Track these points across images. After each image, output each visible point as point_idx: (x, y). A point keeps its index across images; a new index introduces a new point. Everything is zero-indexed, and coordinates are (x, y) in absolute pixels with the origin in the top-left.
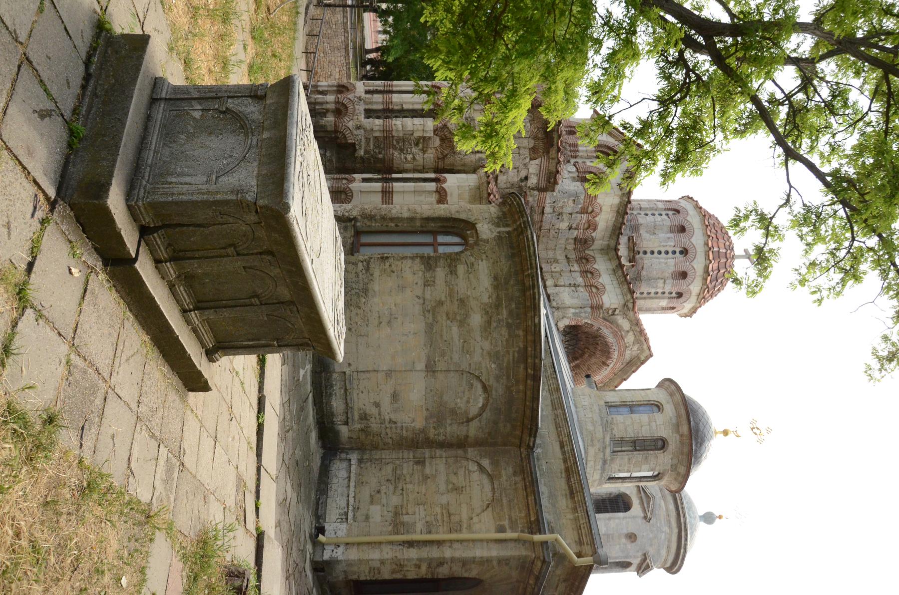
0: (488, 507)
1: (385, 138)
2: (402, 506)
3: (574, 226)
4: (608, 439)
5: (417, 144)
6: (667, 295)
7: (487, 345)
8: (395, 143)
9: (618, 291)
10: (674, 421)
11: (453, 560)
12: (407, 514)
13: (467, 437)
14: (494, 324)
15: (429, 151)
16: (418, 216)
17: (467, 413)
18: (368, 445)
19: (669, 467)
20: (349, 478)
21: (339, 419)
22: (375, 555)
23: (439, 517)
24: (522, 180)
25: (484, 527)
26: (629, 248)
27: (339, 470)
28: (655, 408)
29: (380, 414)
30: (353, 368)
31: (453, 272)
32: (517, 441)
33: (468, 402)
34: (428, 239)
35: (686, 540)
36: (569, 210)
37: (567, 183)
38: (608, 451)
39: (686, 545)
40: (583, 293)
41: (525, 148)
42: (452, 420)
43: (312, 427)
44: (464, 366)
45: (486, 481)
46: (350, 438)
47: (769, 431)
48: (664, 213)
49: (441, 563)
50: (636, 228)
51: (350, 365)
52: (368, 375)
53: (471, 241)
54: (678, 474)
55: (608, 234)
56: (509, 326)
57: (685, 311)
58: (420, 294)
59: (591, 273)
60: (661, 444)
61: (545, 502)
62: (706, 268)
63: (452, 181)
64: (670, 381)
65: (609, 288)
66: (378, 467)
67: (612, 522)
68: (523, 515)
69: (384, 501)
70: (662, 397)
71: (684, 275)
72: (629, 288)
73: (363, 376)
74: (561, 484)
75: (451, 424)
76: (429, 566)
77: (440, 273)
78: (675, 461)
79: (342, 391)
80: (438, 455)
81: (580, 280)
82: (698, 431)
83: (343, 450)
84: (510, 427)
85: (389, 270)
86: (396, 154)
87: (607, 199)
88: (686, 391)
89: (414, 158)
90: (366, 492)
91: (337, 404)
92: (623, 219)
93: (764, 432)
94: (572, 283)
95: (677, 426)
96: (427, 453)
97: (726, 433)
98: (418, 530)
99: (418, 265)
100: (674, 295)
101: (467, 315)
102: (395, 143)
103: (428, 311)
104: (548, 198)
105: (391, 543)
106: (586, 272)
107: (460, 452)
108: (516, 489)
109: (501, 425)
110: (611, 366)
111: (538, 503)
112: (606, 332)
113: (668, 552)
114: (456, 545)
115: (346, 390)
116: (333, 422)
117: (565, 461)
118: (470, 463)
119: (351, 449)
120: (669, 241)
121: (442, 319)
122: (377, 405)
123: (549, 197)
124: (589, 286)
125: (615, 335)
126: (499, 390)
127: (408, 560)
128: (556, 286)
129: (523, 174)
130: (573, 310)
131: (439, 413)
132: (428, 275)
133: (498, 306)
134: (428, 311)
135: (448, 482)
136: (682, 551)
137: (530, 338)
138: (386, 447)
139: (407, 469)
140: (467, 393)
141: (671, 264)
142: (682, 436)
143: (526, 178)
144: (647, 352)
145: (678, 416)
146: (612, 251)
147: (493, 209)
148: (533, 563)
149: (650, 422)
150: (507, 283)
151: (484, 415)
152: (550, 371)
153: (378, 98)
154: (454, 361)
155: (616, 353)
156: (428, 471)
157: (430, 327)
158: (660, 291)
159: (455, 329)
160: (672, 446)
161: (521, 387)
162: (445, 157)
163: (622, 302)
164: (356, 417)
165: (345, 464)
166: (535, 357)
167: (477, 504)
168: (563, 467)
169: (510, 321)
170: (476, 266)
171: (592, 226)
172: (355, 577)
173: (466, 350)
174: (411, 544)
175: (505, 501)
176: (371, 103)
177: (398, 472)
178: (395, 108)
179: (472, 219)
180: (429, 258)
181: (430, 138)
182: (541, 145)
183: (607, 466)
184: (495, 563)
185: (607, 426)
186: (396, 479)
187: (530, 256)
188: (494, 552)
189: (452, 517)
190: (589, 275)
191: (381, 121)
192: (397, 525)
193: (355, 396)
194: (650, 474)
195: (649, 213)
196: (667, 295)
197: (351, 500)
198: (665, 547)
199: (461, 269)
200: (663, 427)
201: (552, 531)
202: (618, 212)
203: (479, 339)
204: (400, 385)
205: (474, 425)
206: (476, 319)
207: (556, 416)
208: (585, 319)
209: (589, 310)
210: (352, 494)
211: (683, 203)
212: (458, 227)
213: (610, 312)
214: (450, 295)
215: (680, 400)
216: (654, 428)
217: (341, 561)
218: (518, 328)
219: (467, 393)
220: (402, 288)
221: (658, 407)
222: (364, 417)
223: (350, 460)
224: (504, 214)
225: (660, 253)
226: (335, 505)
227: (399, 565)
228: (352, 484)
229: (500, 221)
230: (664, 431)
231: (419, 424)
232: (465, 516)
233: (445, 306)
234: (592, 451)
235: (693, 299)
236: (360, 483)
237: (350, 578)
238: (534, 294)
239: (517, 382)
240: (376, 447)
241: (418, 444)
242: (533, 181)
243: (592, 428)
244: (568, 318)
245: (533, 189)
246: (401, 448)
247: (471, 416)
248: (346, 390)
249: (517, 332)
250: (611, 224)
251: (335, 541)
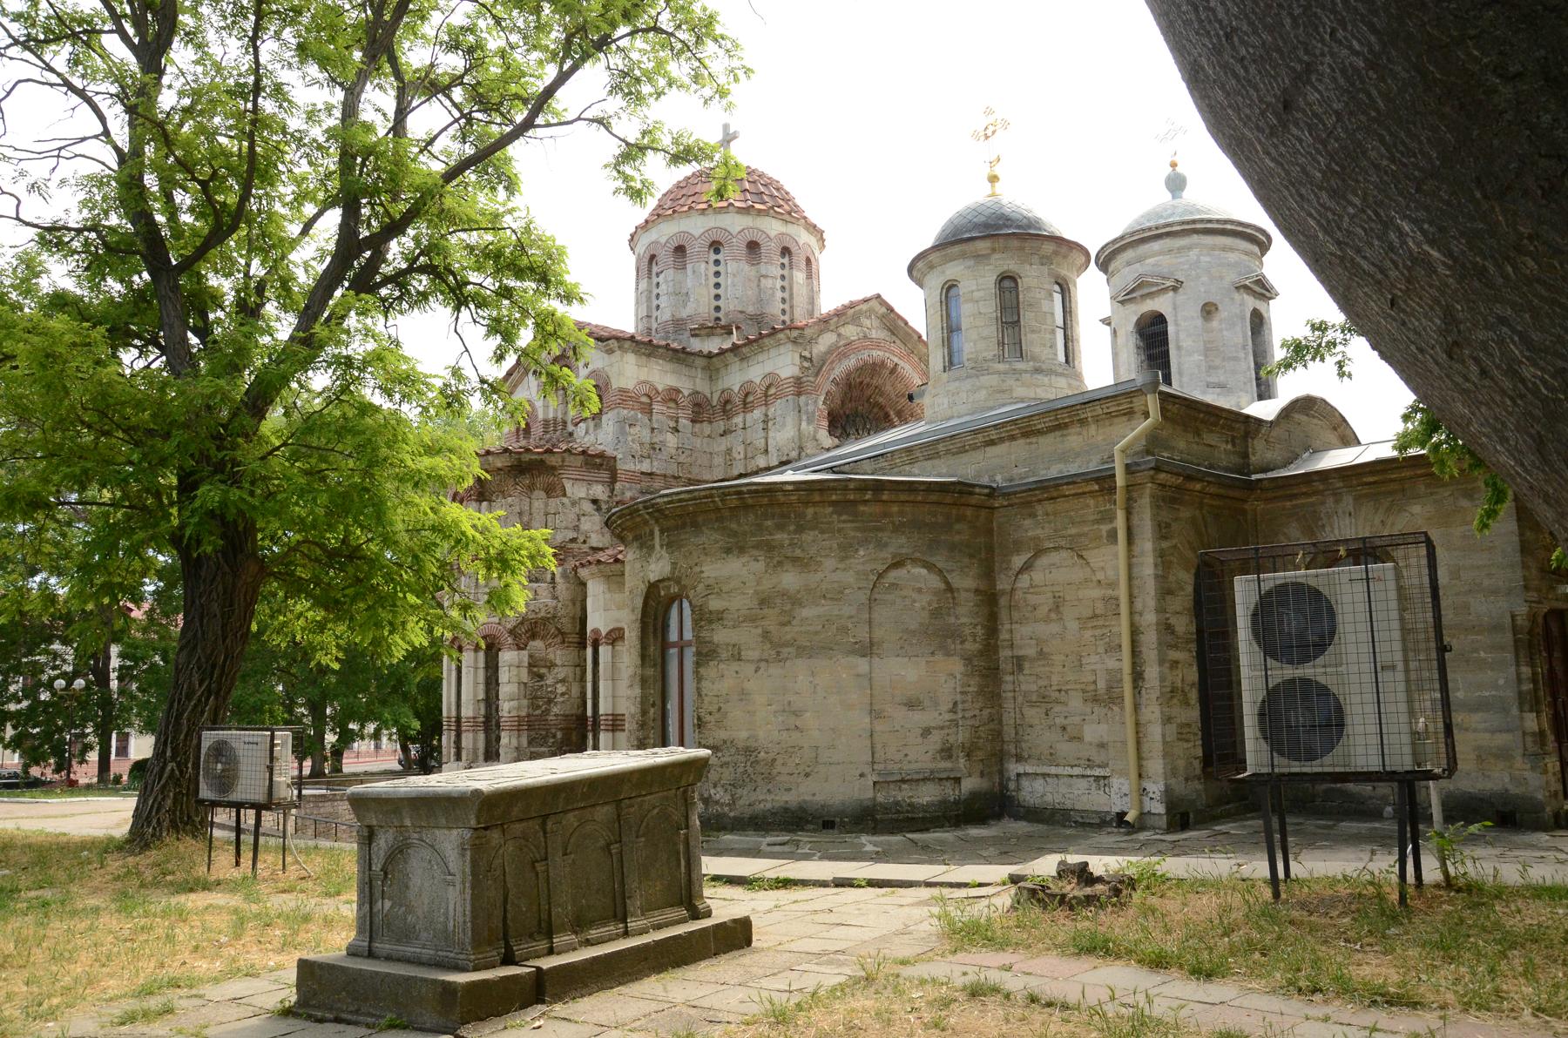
0: (1081, 557)
1: (530, 728)
2: (1084, 691)
3: (672, 424)
4: (1001, 367)
5: (541, 677)
6: (786, 272)
7: (829, 563)
8: (538, 712)
9: (773, 352)
10: (971, 262)
11: (1160, 610)
12: (1095, 682)
13: (977, 591)
14: (798, 552)
15: (551, 656)
16: (639, 671)
17: (936, 593)
18: (994, 746)
19: (1045, 268)
20: (1044, 775)
21: (950, 793)
22: (1155, 732)
23: (1098, 632)
24: (599, 509)
25: (1110, 560)
26: (708, 335)
27: (1034, 792)
28: (953, 292)
29: (942, 728)
30: (867, 770)
31: (719, 617)
32: (983, 513)
33: (920, 590)
34: (674, 651)
35: (1210, 221)
36: (645, 435)
37: (602, 438)
38: (1020, 366)
39: (1218, 221)
40: (777, 408)
41: (547, 505)
43: (959, 833)
44: (862, 597)
45: (1044, 561)
46: (982, 775)
47: (989, 111)
48: (655, 280)
49: (1166, 628)
50: (678, 324)
51: (862, 775)
52: (879, 747)
53: (674, 589)
54: (1056, 253)
55: (685, 370)
56: (800, 529)
57: (812, 241)
58: (752, 667)
59: (747, 395)
60: (1008, 283)
61: (1073, 469)
62: (740, 211)
63: (597, 621)
64: (911, 269)
65: (768, 369)
66: (1029, 730)
67: (1184, 345)
68: (1092, 502)
69: (1077, 719)
70: (936, 281)
71: (753, 246)
72: (768, 335)
73: (879, 755)
74: (1046, 443)
75: (957, 617)
76: (1175, 647)
77: (721, 635)
78: (1035, 259)
80: (1007, 637)
81: (757, 414)
82: (986, 226)
83: (1003, 787)
84: (964, 524)
85: (717, 716)
86: (555, 710)
87: (629, 372)
88: (928, 242)
89: (563, 681)
90: (1065, 749)
91: (927, 795)
92: (659, 346)
93: (991, 119)
94: (762, 425)
95: (979, 258)
96: (1005, 653)
97: (993, 179)
98: (1116, 665)
99: (709, 671)
100: (786, 261)
101: (784, 594)
102: (538, 712)
103: (778, 653)
104: (626, 467)
105: (1137, 707)
106: (745, 403)
107: (1003, 601)
108: (1055, 514)
109: (957, 538)
110: (896, 360)
111: (1072, 480)
112: (839, 370)
113: (1232, 249)
114: (1138, 605)
115: (903, 781)
116: (957, 802)
117: (1012, 438)
118: (1019, 585)
119: (1001, 772)
120: (698, 274)
121: (789, 633)
122: (926, 732)
123: (625, 465)
124: (767, 399)
125: (844, 355)
126: (900, 544)
127: (1162, 679)
128: (766, 451)
129: (588, 507)
130: (804, 424)
131: (939, 634)
132: (724, 655)
133: (770, 548)
134: (778, 653)
135: (1047, 620)
136: (1229, 227)
137: (817, 497)
138: (996, 719)
139: (1028, 684)
140: (904, 593)
141: (735, 268)
142: (994, 250)
143: (595, 502)
144: (874, 303)
145: (963, 256)
146: (712, 363)
147: (630, 555)
148: (1163, 486)
149: (972, 300)
150: (735, 534)
151: (940, 565)
152: (882, 463)
153: (467, 740)
154: (853, 613)
155: (875, 353)
156: (1031, 652)
157: (803, 651)
158: (779, 283)
159: (806, 612)
160: (1010, 264)
161: (895, 509)
162: (560, 632)
163: (790, 346)
164: (948, 764)
165: (1025, 783)
166: (846, 489)
167: (1078, 574)
168: (1021, 441)
169: (792, 528)
170: (711, 582)
171: (672, 396)
172: (1197, 765)
173: (837, 595)
174: (1137, 676)
175: (1073, 531)
176: (475, 750)
177: (1034, 698)
178: (483, 712)
179: (643, 588)
180: (698, 653)
181: (531, 656)
182: (541, 480)
184: (1165, 545)
185: (979, 369)
186: (1043, 700)
187: (695, 499)
188: (1146, 546)
189: (1098, 612)
190: (750, 398)
191: (503, 734)
192: (1111, 698)
193: (914, 766)
194: (1058, 298)
195: (655, 303)
196: (786, 272)
197: (1077, 771)
198: (1223, 254)
199: (715, 604)
200: (981, 281)
201: (1111, 458)
202: (649, 355)
203: (820, 575)
205: (956, 580)
206: (790, 579)
207: (948, 452)
208: (818, 405)
209: (803, 399)
210: (1068, 771)
211: (641, 249)
212: (655, 609)
213: (806, 364)
214: (754, 621)
215: (938, 254)
216: (981, 294)
217: (1166, 785)
218: (802, 516)
219: (904, 593)
220: (744, 695)
221: (950, 287)
222: (947, 752)
223: (1019, 775)
224: (636, 538)
225: (717, 285)
226: (1083, 796)
227: (1172, 694)
228: (1053, 770)
229: (645, 544)
230: (990, 279)
231: (957, 666)
232: (1096, 593)
233: (771, 628)
234: (1020, 391)
235: (791, 229)
236: (1053, 759)
237: (1198, 771)
238: (750, 492)
239: (885, 515)
240: (998, 735)
241: (990, 668)
242: (599, 491)
243: (984, 392)
244: (816, 432)
245: (612, 491)
246: (999, 696)
247: (943, 586)
248: (903, 781)
249: (809, 517)
250: (669, 366)
251: (1135, 795)
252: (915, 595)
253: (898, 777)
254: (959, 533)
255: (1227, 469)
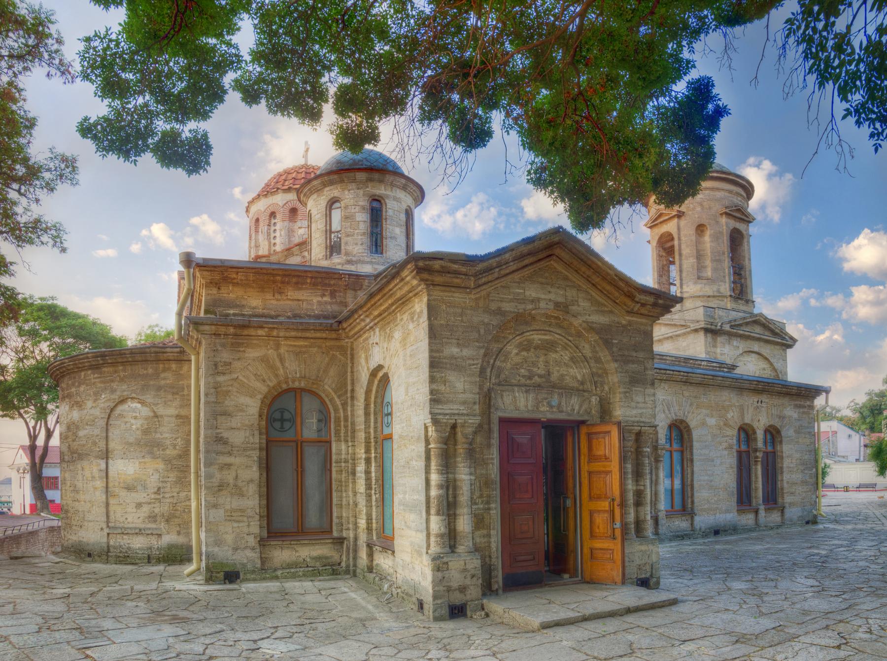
29: (150, 503)
33: (135, 418)
42: (156, 432)
79: (125, 537)
91: (138, 543)
109: (163, 382)
122: (139, 505)
127: (209, 476)
140: (126, 420)
172: (252, 541)
183: (354, 259)
184: (221, 379)
193: (131, 526)
204: (119, 483)
205: (161, 411)
222: (153, 518)
231: (161, 466)
247: (151, 414)
252: (133, 421)
253: (120, 531)
254: (164, 379)
255: (317, 317)
